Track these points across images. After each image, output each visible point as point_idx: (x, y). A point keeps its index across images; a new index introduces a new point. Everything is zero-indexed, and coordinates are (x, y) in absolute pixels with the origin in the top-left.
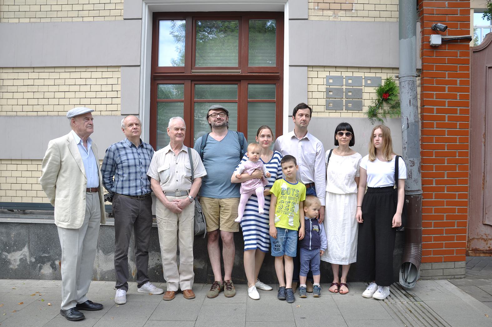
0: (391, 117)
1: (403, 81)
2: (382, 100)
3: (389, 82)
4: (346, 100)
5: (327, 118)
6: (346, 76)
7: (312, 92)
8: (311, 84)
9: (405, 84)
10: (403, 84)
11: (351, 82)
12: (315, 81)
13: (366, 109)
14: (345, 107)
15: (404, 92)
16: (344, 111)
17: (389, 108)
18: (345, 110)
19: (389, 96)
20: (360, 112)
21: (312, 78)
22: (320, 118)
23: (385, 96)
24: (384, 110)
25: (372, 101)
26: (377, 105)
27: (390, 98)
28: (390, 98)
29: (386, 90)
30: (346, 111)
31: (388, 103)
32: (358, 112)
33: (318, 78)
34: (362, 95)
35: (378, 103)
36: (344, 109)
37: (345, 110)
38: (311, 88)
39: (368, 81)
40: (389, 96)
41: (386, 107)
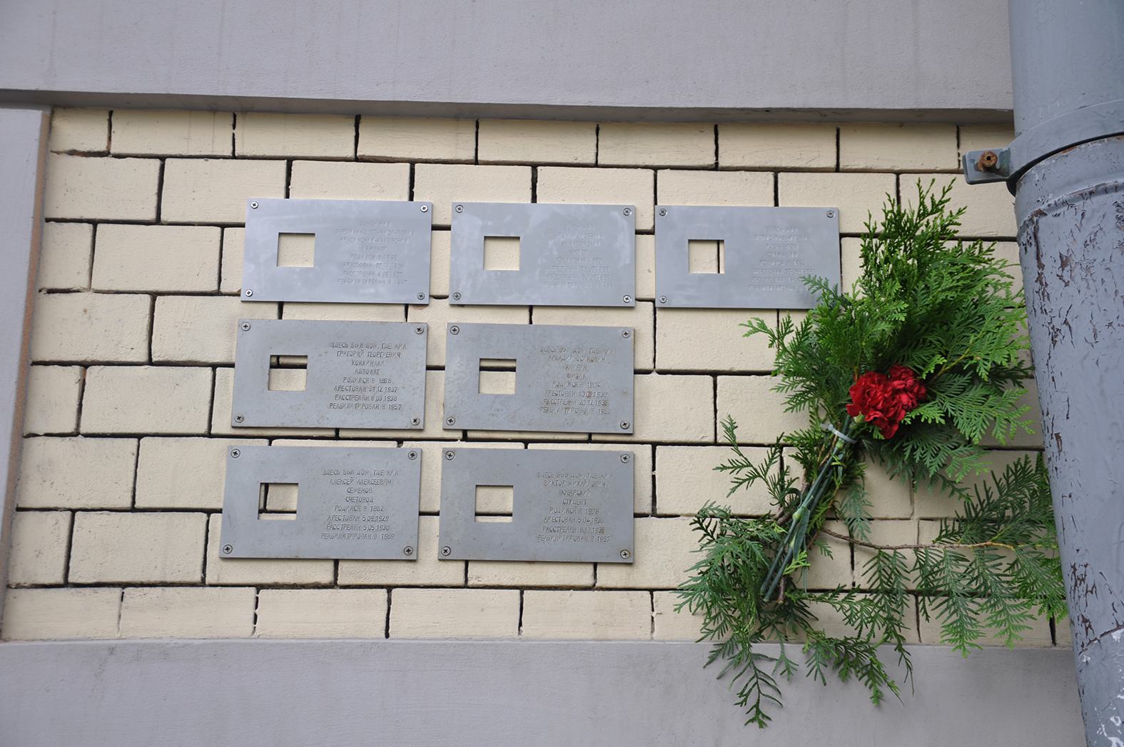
0: (959, 631)
1: (1064, 196)
2: (855, 451)
3: (907, 244)
4: (448, 454)
5: (217, 652)
6: (459, 208)
7: (85, 365)
8: (81, 282)
9: (1090, 227)
10: (1058, 235)
11: (516, 268)
12: (131, 257)
13: (674, 553)
14: (444, 534)
15: (1082, 329)
16: (430, 568)
17: (930, 532)
18: (446, 557)
19: (927, 390)
20: (608, 576)
21: (94, 223)
22: (163, 652)
23: (879, 393)
24: (880, 555)
25: (727, 454)
26: (796, 504)
27: (931, 413)
28: (931, 413)
29: (884, 326)
30: (453, 573)
31: (916, 477)
32: (582, 575)
33: (158, 221)
34: (630, 395)
35: (808, 476)
36: (430, 552)
37: (446, 557)
38: (67, 330)
39: (696, 248)
40: (922, 400)
41: (898, 520)
